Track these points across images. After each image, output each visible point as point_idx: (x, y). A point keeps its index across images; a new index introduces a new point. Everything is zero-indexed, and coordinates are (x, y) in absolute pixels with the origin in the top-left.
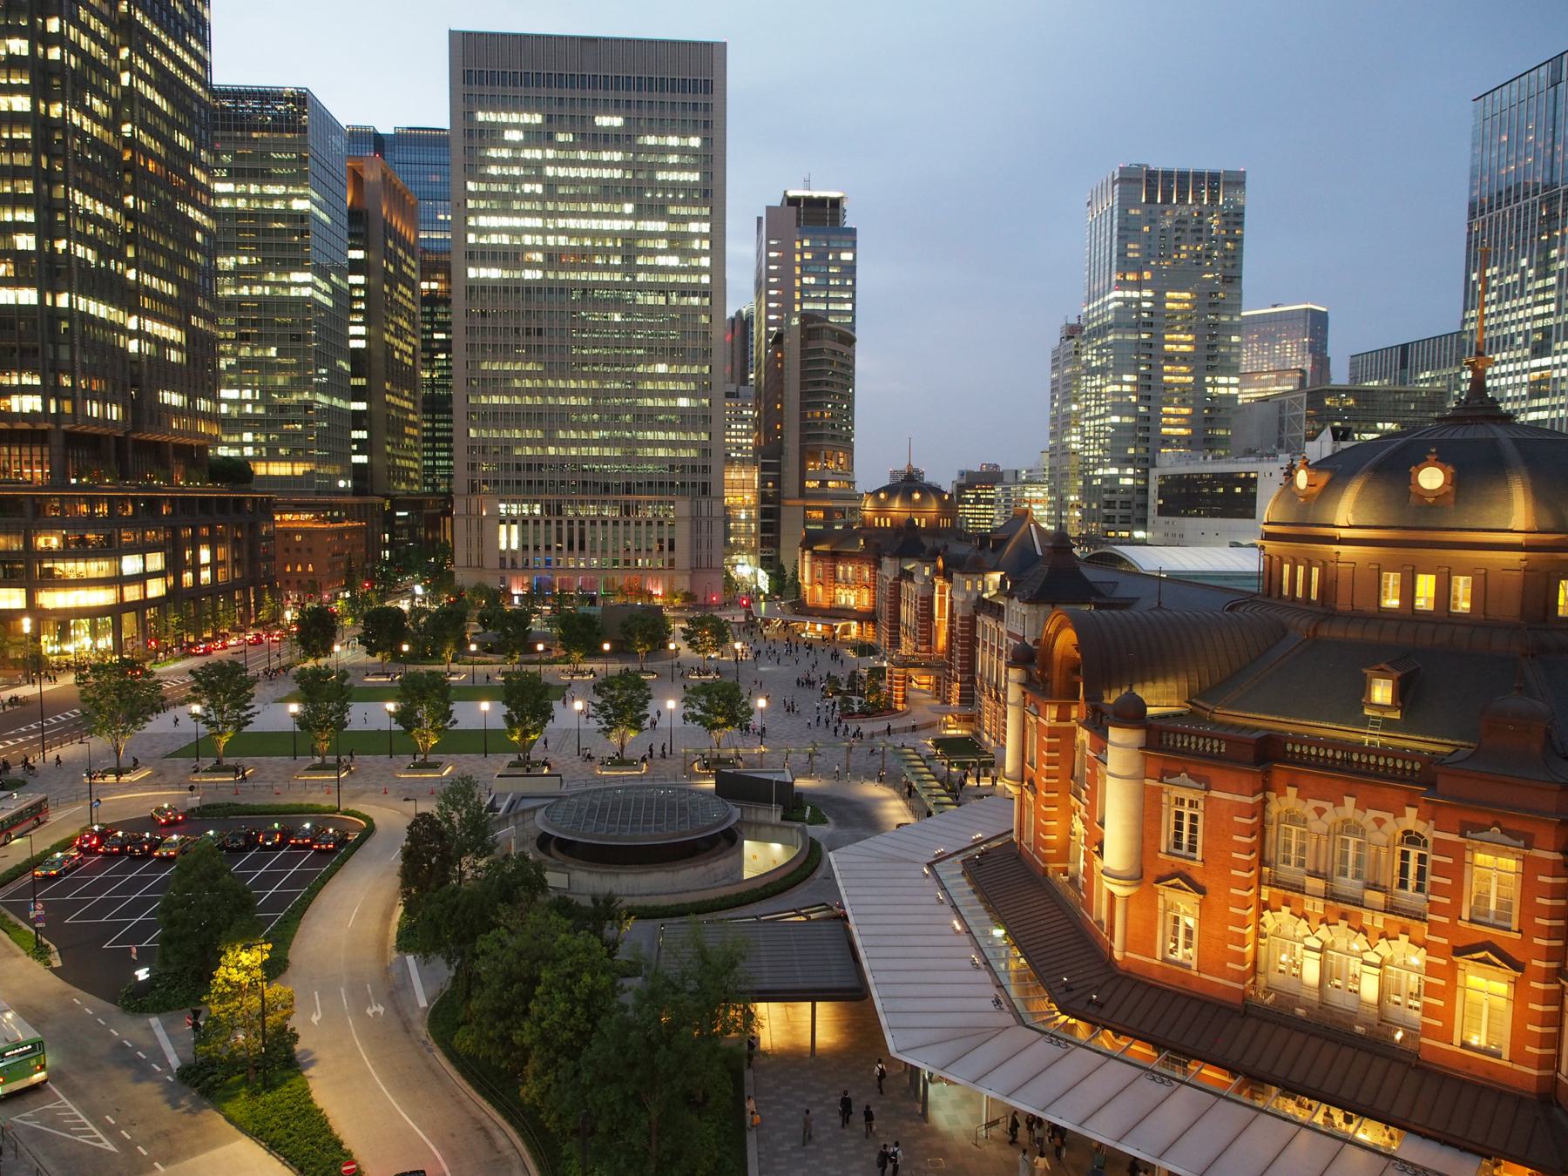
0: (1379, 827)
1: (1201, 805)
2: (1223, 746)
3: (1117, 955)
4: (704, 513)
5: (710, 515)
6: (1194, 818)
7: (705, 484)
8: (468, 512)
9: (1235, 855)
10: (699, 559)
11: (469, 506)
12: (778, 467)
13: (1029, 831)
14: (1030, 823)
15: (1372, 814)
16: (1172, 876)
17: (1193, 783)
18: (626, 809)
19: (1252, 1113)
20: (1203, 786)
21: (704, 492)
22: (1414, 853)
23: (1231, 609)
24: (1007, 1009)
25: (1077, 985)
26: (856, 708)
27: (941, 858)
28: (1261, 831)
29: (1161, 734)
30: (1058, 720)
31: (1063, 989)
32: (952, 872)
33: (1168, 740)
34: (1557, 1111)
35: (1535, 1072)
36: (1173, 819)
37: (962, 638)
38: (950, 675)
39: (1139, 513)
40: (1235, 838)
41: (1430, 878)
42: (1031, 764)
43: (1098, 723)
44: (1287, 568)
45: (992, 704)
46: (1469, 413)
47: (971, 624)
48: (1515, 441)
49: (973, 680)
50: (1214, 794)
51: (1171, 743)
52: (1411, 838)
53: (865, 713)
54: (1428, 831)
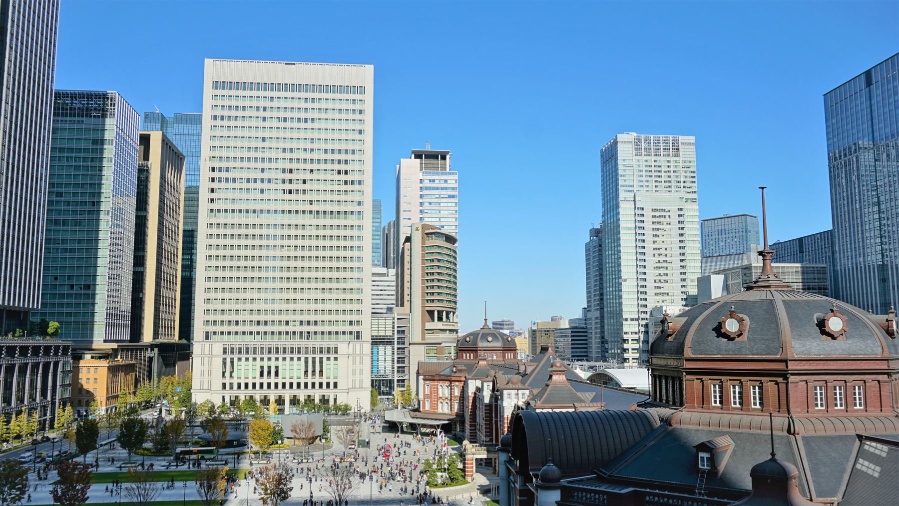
4: (358, 352)
5: (361, 353)
7: (358, 332)
8: (203, 354)
11: (203, 349)
21: (358, 338)
53: (444, 484)
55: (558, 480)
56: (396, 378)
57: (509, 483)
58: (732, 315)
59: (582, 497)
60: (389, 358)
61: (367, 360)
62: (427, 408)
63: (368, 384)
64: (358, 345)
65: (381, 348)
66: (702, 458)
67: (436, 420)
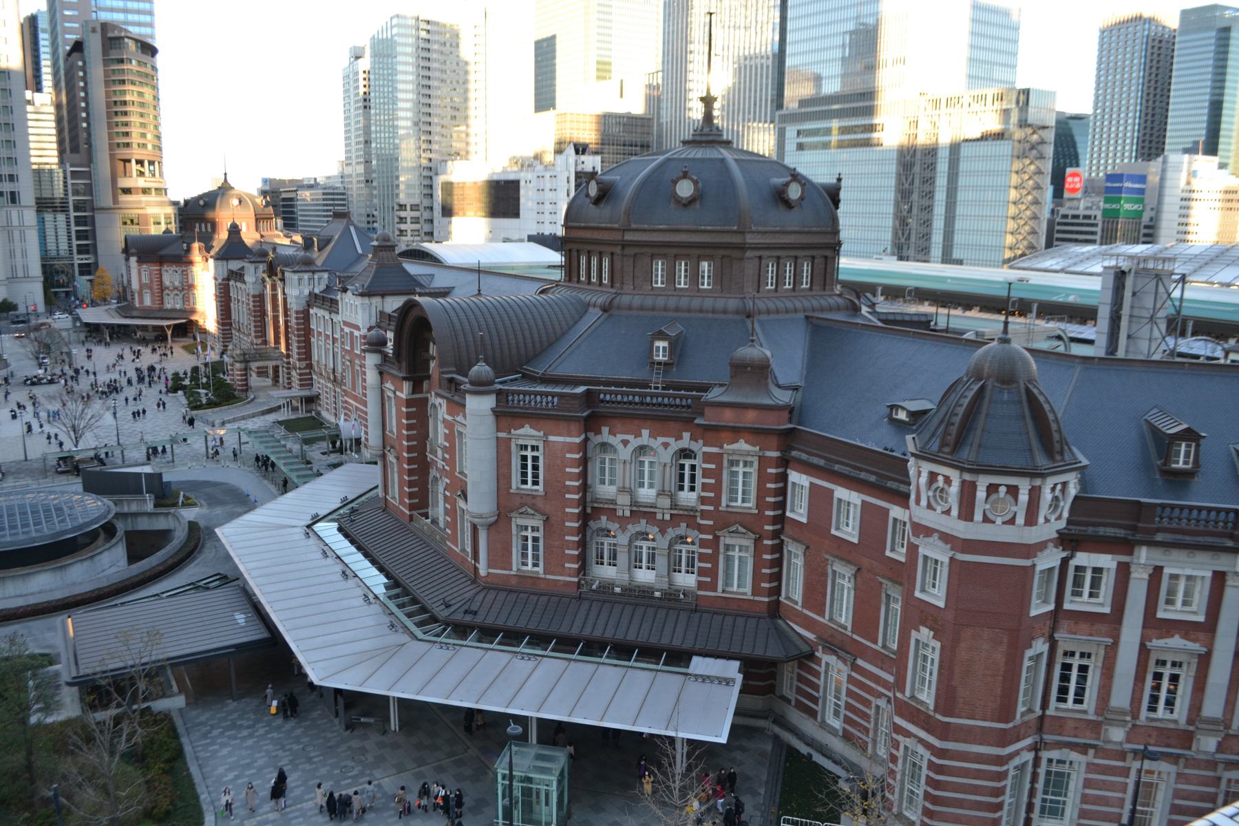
0: (666, 448)
1: (541, 448)
2: (556, 399)
3: (483, 572)
4: (15, 222)
6: (535, 459)
7: (13, 193)
9: (568, 483)
10: (13, 269)
12: (88, 175)
13: (393, 487)
14: (393, 480)
15: (661, 440)
16: (522, 505)
17: (534, 432)
18: (11, 515)
19: (595, 666)
20: (541, 433)
22: (687, 463)
23: (542, 292)
24: (401, 630)
25: (454, 601)
26: (204, 401)
27: (317, 519)
28: (584, 462)
29: (507, 396)
30: (414, 392)
31: (443, 607)
32: (328, 530)
33: (513, 401)
34: (780, 622)
35: (766, 600)
36: (519, 462)
37: (298, 330)
38: (289, 363)
39: (426, 215)
40: (568, 470)
41: (700, 480)
42: (391, 431)
43: (455, 392)
44: (583, 260)
45: (330, 385)
46: (704, 138)
47: (305, 316)
48: (736, 160)
49: (310, 366)
50: (551, 438)
51: (516, 402)
52: (686, 453)
53: (211, 404)
54: (699, 447)
55: (492, 383)
56: (77, 262)
57: (382, 392)
58: (685, 175)
59: (519, 401)
60: (62, 232)
61: (33, 237)
62: (148, 301)
63: (36, 269)
64: (14, 213)
65: (49, 217)
66: (658, 348)
67: (162, 318)
